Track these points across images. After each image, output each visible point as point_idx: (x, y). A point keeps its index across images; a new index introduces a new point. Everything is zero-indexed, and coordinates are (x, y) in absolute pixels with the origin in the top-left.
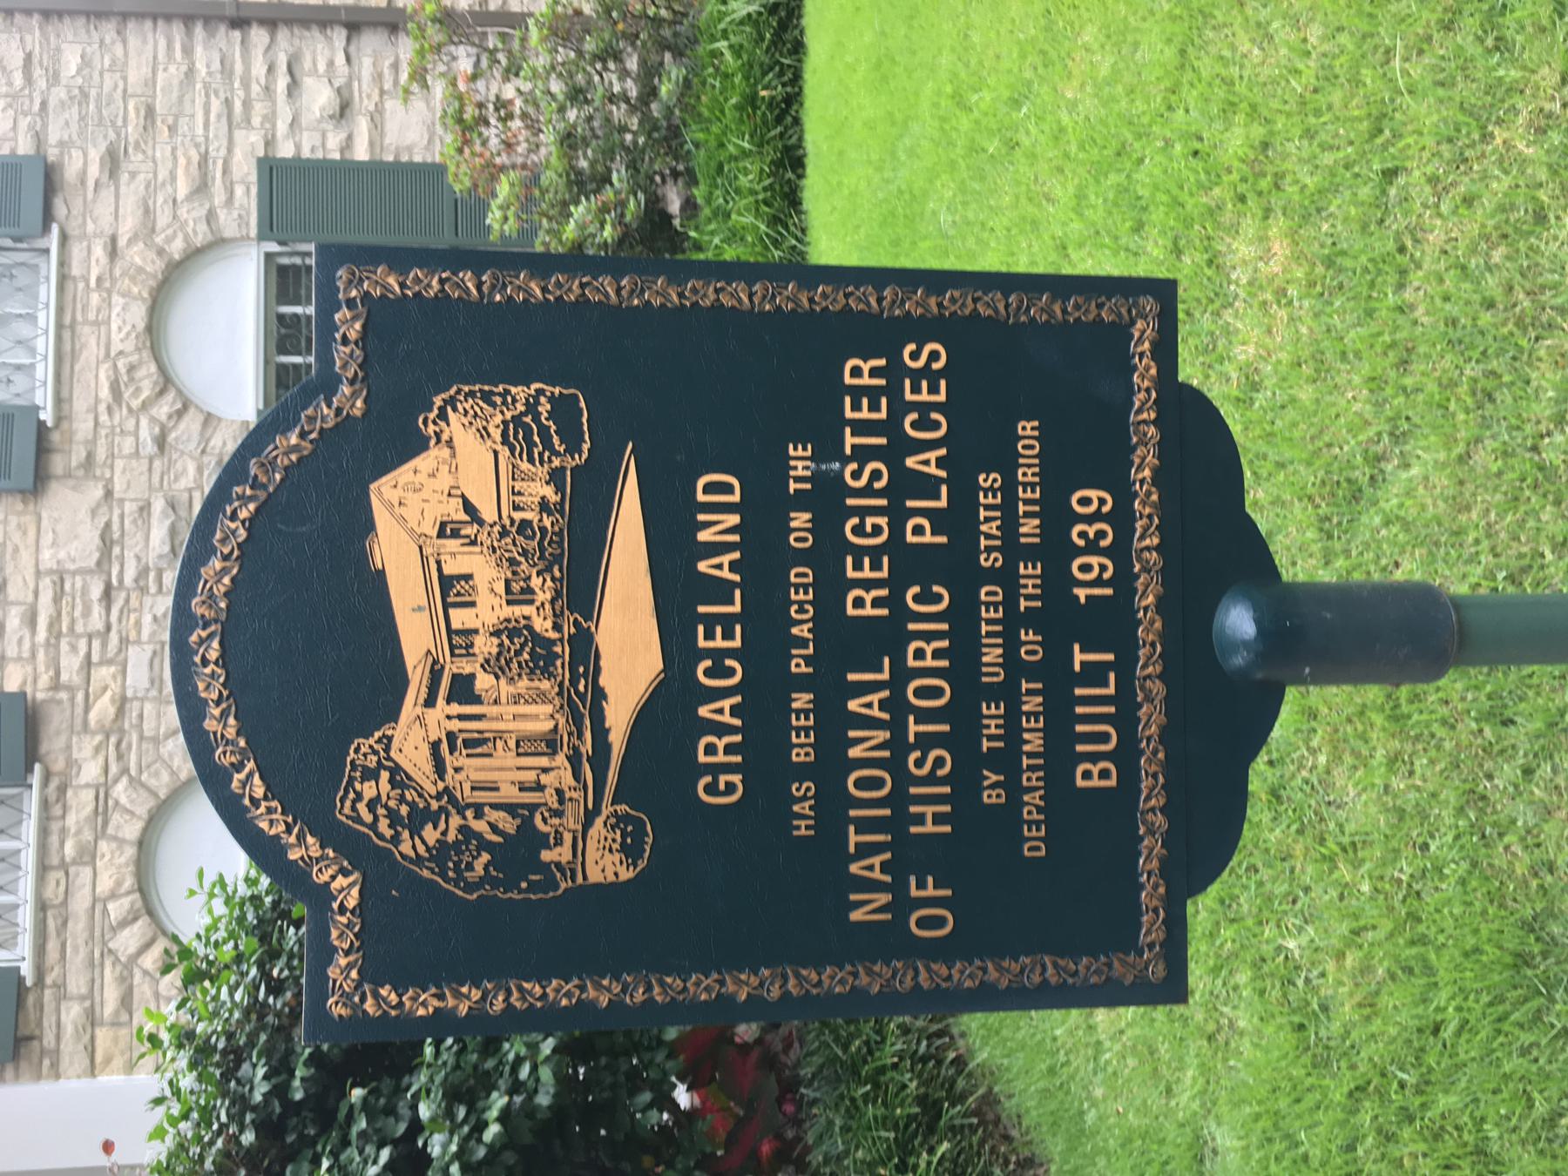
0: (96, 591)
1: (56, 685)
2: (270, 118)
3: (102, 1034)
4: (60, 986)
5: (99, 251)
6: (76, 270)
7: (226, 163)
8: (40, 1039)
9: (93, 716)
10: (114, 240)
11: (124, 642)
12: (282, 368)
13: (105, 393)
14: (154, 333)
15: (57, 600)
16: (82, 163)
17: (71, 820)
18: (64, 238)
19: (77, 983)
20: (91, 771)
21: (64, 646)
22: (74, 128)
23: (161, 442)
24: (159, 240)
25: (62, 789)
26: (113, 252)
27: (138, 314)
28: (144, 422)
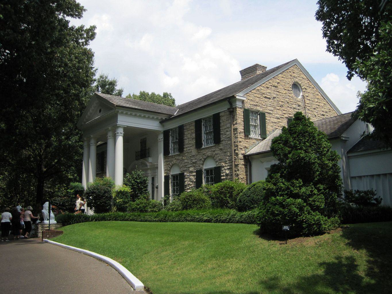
0: (191, 156)
1: (185, 153)
2: (226, 166)
4: (169, 158)
5: (214, 149)
6: (213, 147)
7: (222, 162)
8: (166, 157)
9: (183, 157)
10: (215, 151)
11: (188, 159)
12: (209, 170)
13: (204, 153)
14: (208, 157)
15: (190, 152)
17: (177, 157)
18: (215, 146)
19: (169, 160)
21: (187, 153)
22: (224, 144)
23: (200, 160)
24: (215, 156)
25: (179, 156)
26: (214, 151)
27: (210, 155)
28: (202, 157)
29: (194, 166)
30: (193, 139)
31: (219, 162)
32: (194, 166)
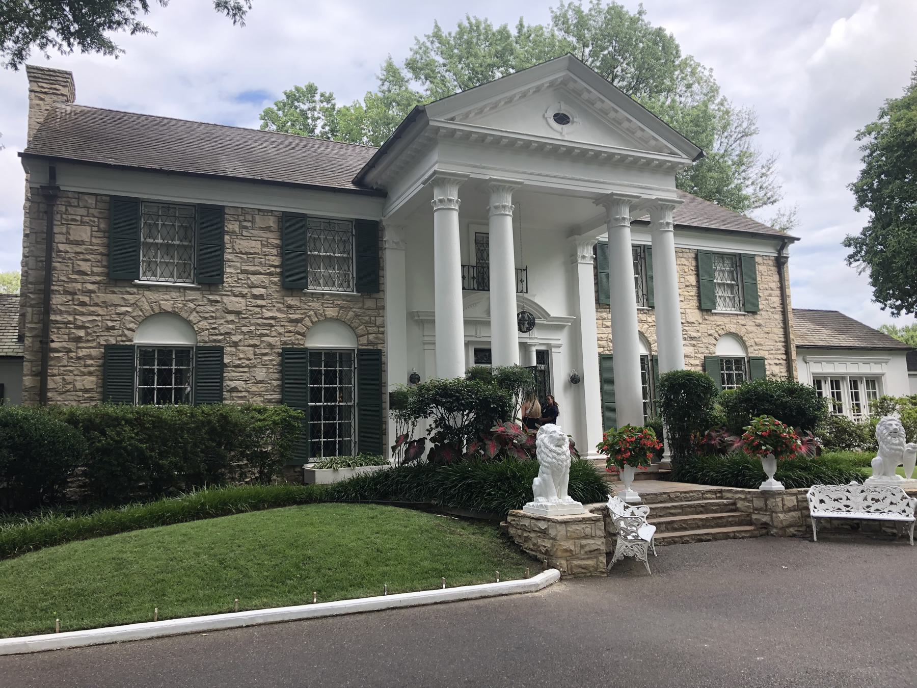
3: (600, 321)
16: (759, 319)
20: (650, 320)
23: (710, 335)
27: (733, 330)
29: (694, 346)
30: (687, 286)
31: (756, 348)
32: (694, 346)
